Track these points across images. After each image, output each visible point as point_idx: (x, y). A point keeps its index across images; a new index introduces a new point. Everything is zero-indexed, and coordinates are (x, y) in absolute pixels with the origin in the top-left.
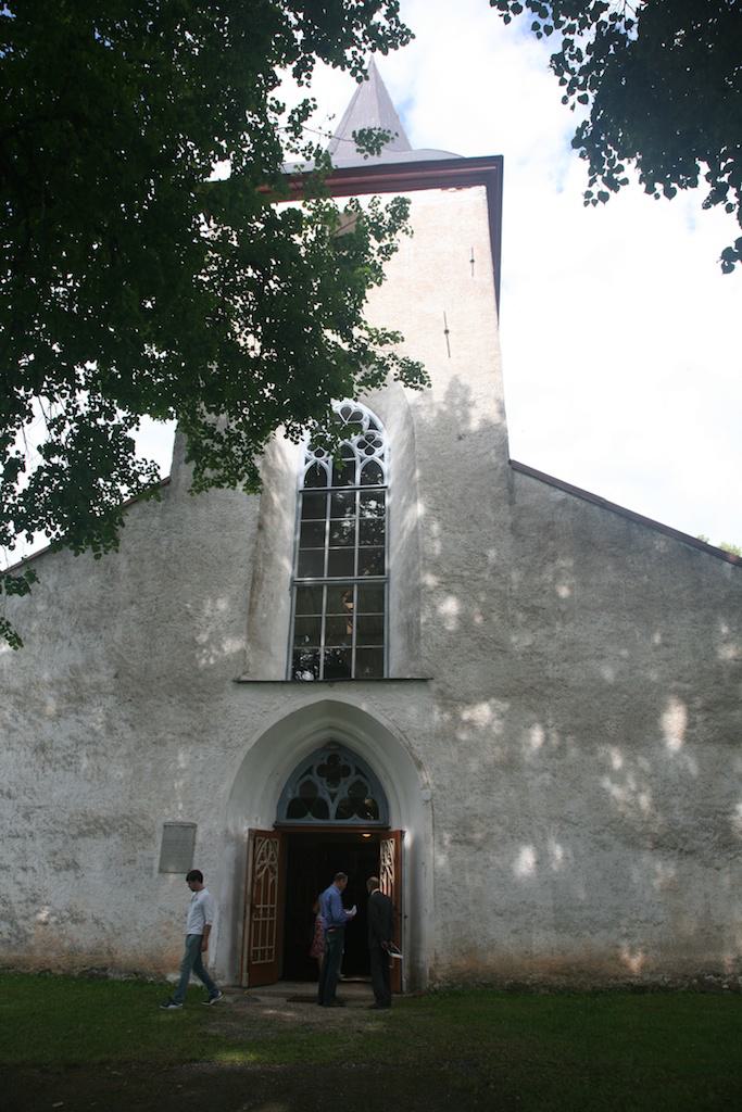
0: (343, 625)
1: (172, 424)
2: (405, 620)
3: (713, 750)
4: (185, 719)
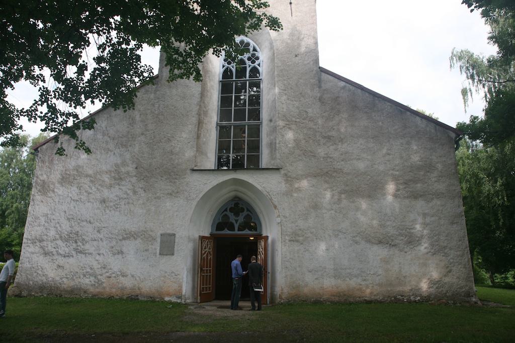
0: (240, 144)
1: (159, 48)
2: (269, 142)
3: (407, 201)
4: (169, 187)
